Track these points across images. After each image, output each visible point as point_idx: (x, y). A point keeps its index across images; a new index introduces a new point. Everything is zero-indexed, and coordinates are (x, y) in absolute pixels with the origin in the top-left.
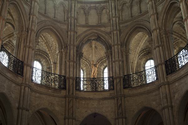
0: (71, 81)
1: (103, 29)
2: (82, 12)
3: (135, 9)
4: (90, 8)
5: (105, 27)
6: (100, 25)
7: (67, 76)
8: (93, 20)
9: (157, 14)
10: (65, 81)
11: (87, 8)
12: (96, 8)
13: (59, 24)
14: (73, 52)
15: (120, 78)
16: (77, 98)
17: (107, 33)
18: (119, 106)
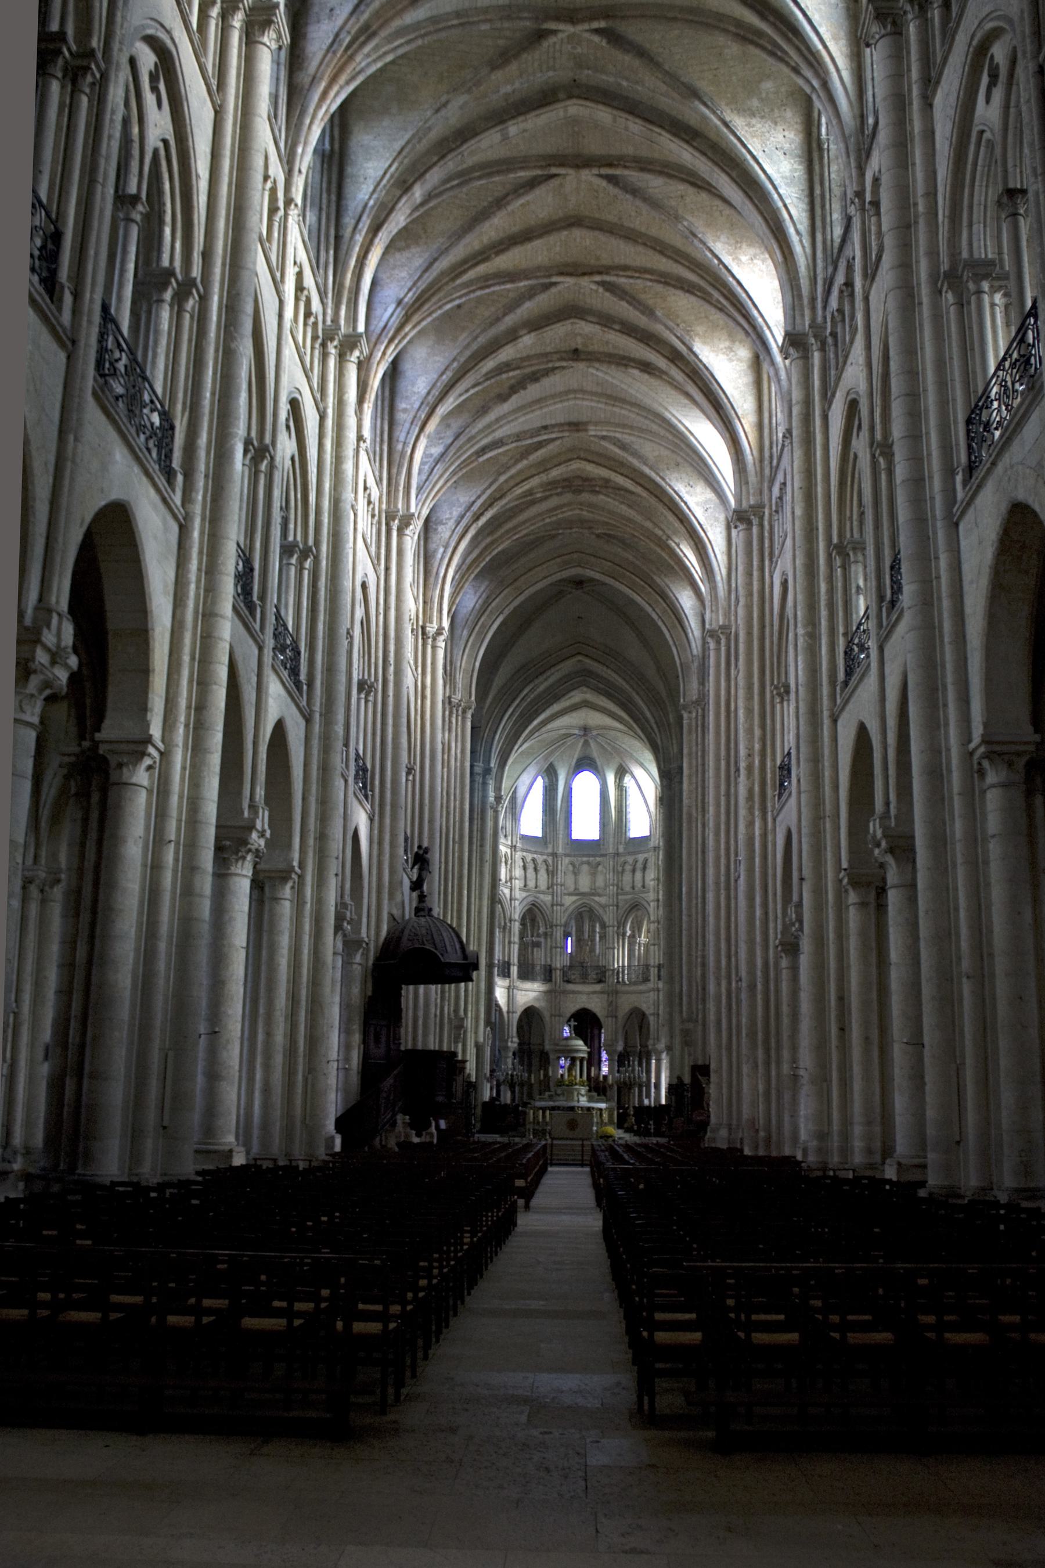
0: (558, 972)
1: (597, 898)
2: (571, 868)
3: (638, 875)
4: (582, 863)
5: (599, 895)
6: (594, 892)
7: (553, 966)
8: (585, 883)
9: (658, 900)
10: (551, 971)
11: (577, 864)
12: (588, 863)
13: (542, 896)
14: (559, 933)
15: (613, 970)
16: (565, 992)
17: (601, 905)
18: (610, 1004)
